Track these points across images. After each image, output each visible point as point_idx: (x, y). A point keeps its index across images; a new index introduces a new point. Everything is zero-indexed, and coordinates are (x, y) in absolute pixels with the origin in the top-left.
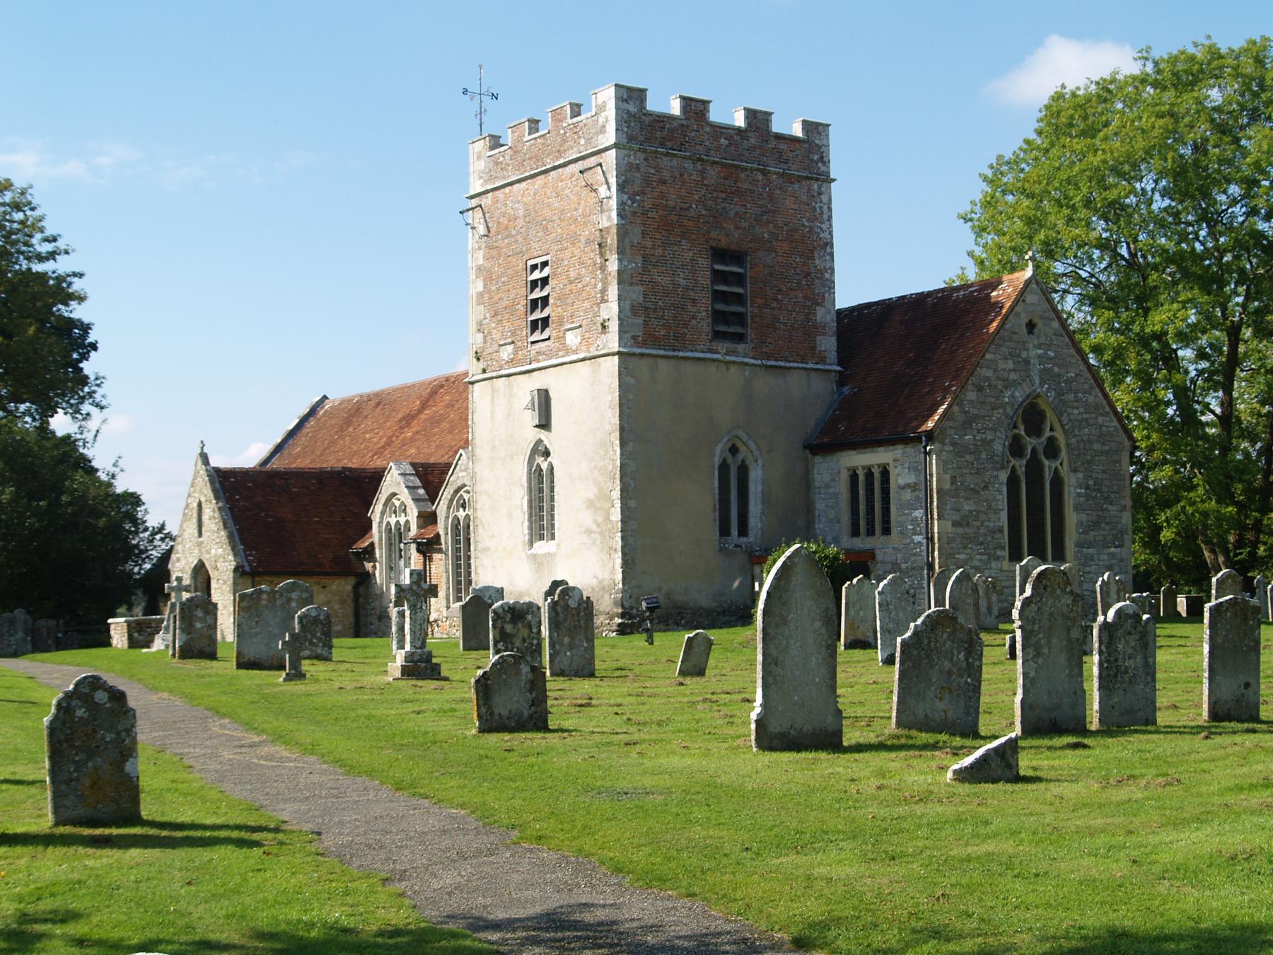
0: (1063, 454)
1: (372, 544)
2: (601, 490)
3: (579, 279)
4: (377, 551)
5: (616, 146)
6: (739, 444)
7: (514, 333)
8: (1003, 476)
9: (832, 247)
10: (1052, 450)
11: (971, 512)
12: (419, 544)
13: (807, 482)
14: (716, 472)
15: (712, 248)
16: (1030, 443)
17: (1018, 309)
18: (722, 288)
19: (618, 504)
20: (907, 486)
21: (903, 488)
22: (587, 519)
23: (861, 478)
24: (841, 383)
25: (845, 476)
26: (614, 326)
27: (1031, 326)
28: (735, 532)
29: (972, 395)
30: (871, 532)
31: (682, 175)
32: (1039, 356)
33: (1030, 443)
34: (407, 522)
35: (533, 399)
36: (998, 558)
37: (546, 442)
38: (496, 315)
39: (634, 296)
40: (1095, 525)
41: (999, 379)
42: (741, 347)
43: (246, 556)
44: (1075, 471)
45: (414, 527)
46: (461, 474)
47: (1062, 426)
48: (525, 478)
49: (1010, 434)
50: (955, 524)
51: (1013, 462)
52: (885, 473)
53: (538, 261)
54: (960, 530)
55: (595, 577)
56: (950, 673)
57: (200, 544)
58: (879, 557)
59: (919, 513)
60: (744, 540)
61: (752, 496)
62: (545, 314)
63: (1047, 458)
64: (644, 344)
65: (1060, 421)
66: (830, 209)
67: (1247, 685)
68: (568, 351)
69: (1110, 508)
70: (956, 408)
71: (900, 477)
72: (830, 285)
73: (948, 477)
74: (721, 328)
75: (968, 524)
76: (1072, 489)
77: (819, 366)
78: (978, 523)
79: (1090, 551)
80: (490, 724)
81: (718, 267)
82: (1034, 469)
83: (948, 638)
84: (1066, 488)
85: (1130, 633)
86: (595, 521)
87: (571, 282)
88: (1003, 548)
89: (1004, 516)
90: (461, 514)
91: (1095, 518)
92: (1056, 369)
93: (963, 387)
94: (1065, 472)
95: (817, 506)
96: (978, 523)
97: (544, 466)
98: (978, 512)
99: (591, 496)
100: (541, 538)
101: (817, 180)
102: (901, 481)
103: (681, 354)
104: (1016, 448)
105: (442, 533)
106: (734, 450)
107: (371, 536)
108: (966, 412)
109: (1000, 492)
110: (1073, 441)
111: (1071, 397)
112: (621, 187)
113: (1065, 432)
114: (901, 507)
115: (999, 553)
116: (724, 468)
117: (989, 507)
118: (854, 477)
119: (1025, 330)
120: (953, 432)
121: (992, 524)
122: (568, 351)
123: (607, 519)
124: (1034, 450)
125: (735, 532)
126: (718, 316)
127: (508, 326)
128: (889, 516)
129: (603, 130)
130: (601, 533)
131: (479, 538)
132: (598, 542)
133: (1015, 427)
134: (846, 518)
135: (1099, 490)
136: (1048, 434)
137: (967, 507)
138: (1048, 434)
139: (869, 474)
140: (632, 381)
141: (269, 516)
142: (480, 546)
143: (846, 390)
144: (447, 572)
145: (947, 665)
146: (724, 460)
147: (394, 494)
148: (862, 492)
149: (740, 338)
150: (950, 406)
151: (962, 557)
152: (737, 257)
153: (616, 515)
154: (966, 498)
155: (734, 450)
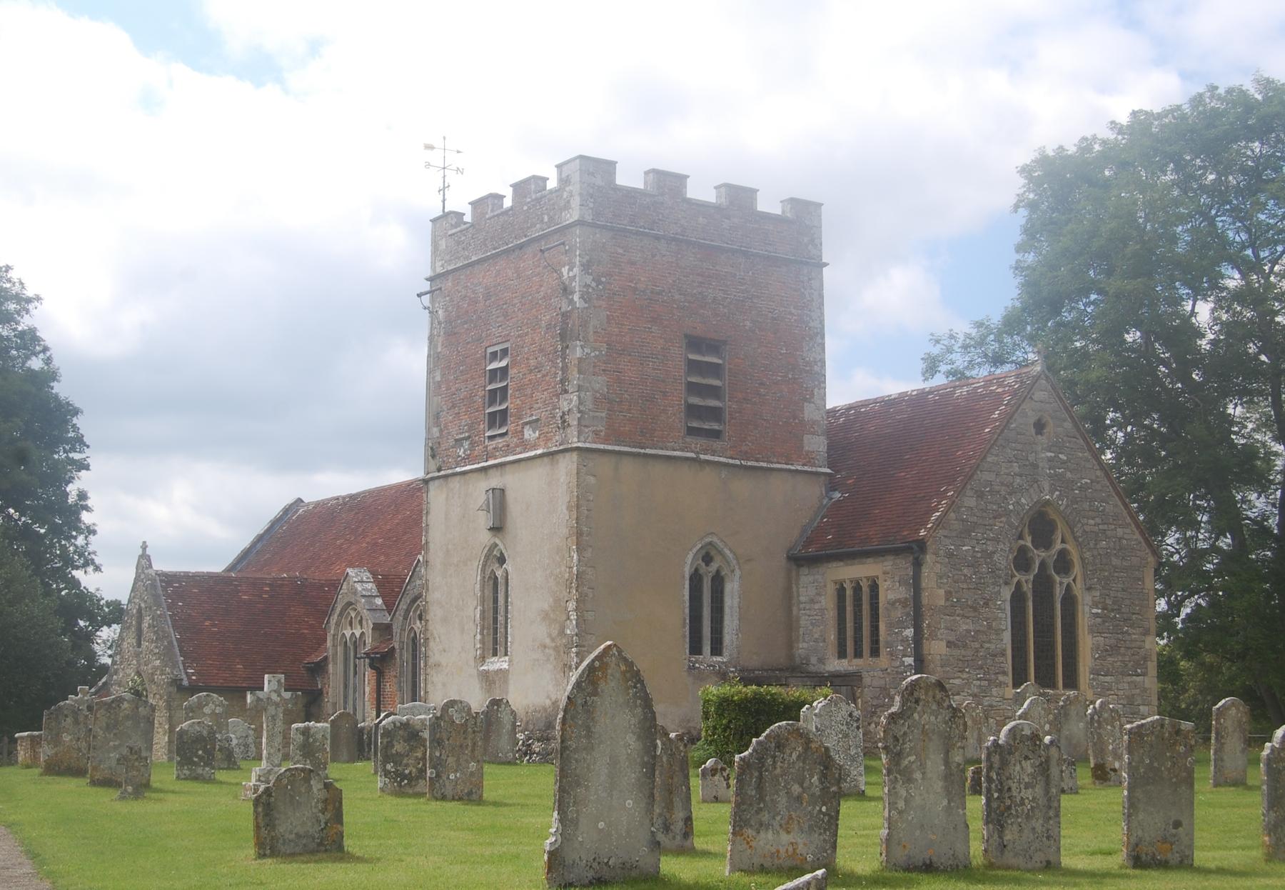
0: (1077, 570)
1: (326, 658)
2: (557, 601)
3: (538, 368)
4: (330, 666)
5: (580, 223)
6: (713, 553)
7: (471, 427)
8: (1007, 593)
9: (823, 337)
10: (1063, 564)
11: (968, 631)
12: (372, 659)
13: (788, 596)
14: (687, 583)
15: (686, 336)
16: (1038, 555)
17: (1023, 406)
18: (693, 379)
19: (573, 617)
20: (899, 600)
21: (893, 603)
22: (541, 632)
23: (849, 592)
24: (832, 487)
25: (831, 589)
26: (573, 420)
27: (1040, 427)
28: (707, 648)
29: (970, 501)
30: (858, 654)
31: (653, 256)
32: (1050, 460)
33: (1038, 555)
34: (363, 634)
35: (488, 499)
36: (1000, 684)
37: (501, 546)
38: (454, 406)
39: (597, 386)
40: (1113, 650)
41: (1002, 484)
42: (717, 445)
43: (185, 669)
44: (1089, 589)
45: (369, 640)
47: (1075, 538)
48: (478, 586)
49: (1015, 548)
50: (950, 644)
51: (1018, 577)
52: (874, 588)
53: (497, 348)
54: (956, 652)
55: (548, 697)
56: (799, 799)
57: (137, 655)
58: (867, 680)
59: (909, 632)
60: (719, 659)
61: (727, 610)
62: (503, 407)
63: (1058, 573)
64: (606, 441)
65: (1073, 532)
66: (821, 296)
67: (1177, 824)
68: (526, 446)
69: (1131, 631)
70: (952, 515)
71: (890, 592)
72: (820, 380)
73: (942, 592)
74: (695, 424)
75: (965, 646)
76: (1087, 609)
77: (806, 468)
78: (977, 645)
79: (1108, 679)
80: (268, 846)
81: (691, 357)
82: (1043, 586)
83: (799, 757)
84: (1080, 608)
85: (1026, 758)
86: (550, 635)
87: (531, 371)
88: (1005, 673)
89: (1007, 637)
90: (418, 625)
91: (1113, 641)
92: (1069, 475)
93: (960, 492)
94: (1078, 589)
95: (802, 623)
96: (977, 645)
97: (499, 573)
98: (977, 632)
99: (546, 607)
100: (495, 654)
101: (807, 263)
102: (891, 596)
103: (648, 451)
104: (1022, 561)
105: (397, 647)
106: (708, 559)
107: (326, 650)
108: (963, 520)
109: (1003, 610)
110: (1087, 555)
111: (1086, 505)
112: (586, 267)
113: (1079, 545)
114: (890, 626)
115: (1001, 678)
116: (696, 579)
117: (990, 627)
118: (841, 592)
119: (1033, 431)
120: (948, 541)
121: (993, 646)
123: (562, 633)
124: (1043, 565)
125: (707, 648)
126: (692, 411)
127: (465, 420)
128: (878, 635)
129: (567, 206)
130: (556, 649)
131: (430, 653)
132: (552, 658)
133: (1021, 537)
134: (832, 637)
135: (1119, 611)
136: (1058, 546)
137: (964, 626)
138: (1058, 546)
139: (857, 589)
140: (592, 480)
141: (214, 625)
142: (431, 661)
143: (837, 495)
144: (401, 689)
145: (796, 789)
146: (696, 570)
147: (349, 604)
148: (849, 609)
149: (716, 435)
150: (945, 514)
151: (957, 681)
152: (714, 347)
154: (964, 616)
155: (708, 559)
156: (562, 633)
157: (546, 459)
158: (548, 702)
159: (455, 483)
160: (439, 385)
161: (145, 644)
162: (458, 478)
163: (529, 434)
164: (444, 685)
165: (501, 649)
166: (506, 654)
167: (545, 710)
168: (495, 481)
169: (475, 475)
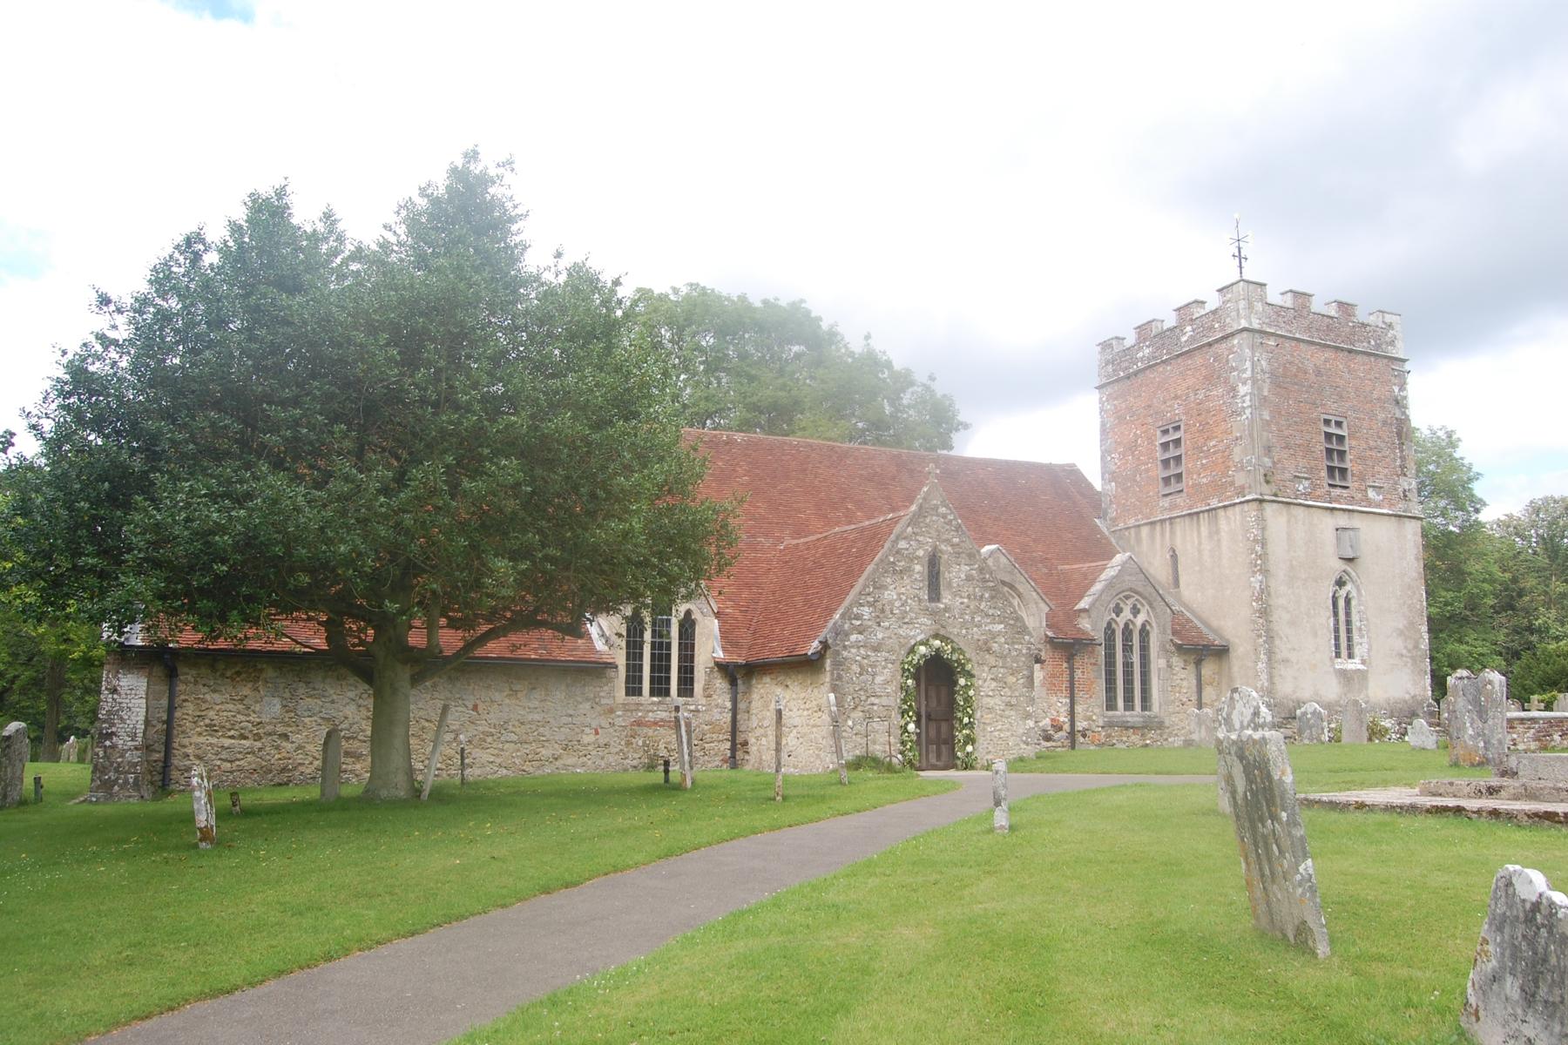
19: (1426, 636)
22: (1399, 644)
57: (933, 614)
68: (1370, 503)
122: (1370, 503)
123: (1416, 647)
130: (1413, 658)
142: (1279, 657)
153: (1425, 644)
156: (1416, 647)
159: (1300, 511)
160: (1268, 423)
161: (947, 598)
163: (1371, 494)
166: (1350, 656)
168: (1343, 520)
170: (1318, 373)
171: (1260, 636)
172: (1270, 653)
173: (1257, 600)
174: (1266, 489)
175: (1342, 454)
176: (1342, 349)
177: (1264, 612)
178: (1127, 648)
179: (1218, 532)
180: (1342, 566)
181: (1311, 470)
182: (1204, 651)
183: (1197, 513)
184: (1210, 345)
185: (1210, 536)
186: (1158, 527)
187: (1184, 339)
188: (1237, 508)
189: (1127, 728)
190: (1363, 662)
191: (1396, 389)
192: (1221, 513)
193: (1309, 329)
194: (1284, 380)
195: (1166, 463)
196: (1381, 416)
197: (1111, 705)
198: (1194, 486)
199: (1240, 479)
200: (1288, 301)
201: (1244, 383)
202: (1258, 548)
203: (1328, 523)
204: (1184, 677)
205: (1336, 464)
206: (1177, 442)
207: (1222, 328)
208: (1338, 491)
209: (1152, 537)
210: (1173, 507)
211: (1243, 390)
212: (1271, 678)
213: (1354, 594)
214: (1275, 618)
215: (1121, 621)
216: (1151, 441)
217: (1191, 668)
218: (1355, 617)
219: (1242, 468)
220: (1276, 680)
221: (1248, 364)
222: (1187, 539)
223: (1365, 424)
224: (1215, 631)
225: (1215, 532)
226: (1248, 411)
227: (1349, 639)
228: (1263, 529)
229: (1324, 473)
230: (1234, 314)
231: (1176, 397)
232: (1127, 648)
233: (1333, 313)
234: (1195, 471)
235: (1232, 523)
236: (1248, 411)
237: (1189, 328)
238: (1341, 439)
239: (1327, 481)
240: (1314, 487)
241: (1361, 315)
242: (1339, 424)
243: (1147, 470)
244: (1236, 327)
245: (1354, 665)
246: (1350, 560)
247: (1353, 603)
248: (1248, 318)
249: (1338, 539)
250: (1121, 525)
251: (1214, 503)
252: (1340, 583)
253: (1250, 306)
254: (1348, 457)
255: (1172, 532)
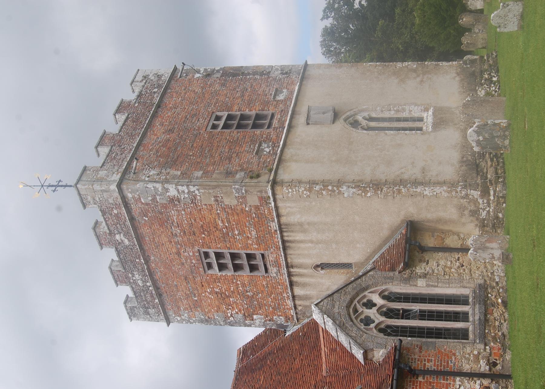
19: (406, 64)
46: (336, 310)
55: (454, 78)
68: (289, 98)
86: (415, 78)
122: (289, 98)
132: (430, 76)
142: (419, 176)
156: (415, 71)
157: (304, 82)
158: (458, 79)
159: (289, 152)
160: (206, 173)
162: (286, 150)
163: (281, 97)
164: (440, 163)
165: (417, 124)
167: (462, 80)
168: (301, 119)
169: (290, 136)
170: (171, 131)
171: (399, 191)
172: (416, 183)
173: (366, 192)
174: (264, 178)
175: (243, 117)
176: (156, 112)
177: (377, 186)
178: (406, 314)
179: (301, 224)
180: (340, 124)
181: (253, 142)
182: (412, 245)
183: (284, 242)
184: (132, 219)
185: (304, 231)
186: (295, 279)
187: (126, 242)
188: (280, 204)
189: (486, 320)
190: (427, 110)
191: (197, 75)
192: (283, 220)
193: (132, 136)
194: (174, 158)
195: (237, 268)
196: (217, 87)
197: (463, 335)
198: (259, 244)
199: (253, 200)
200: (104, 150)
201: (167, 190)
202: (317, 188)
203: (302, 130)
204: (436, 263)
205: (251, 122)
206: (219, 256)
207: (117, 207)
208: (275, 123)
209: (304, 285)
210: (277, 264)
211: (172, 192)
212: (441, 184)
213: (366, 114)
214: (383, 178)
215: (379, 319)
216: (217, 280)
217: (427, 256)
218: (387, 115)
219: (244, 197)
220: (441, 179)
221: (150, 185)
222: (305, 254)
223: (222, 98)
224: (393, 232)
225: (302, 227)
226: (192, 189)
227: (406, 120)
228: (300, 182)
229: (258, 132)
230: (105, 195)
231: (178, 253)
232: (406, 314)
233: (124, 117)
234: (245, 242)
235: (293, 210)
236: (192, 189)
237: (118, 237)
238: (230, 117)
239: (265, 130)
240: (268, 139)
241: (131, 97)
242: (218, 118)
243: (243, 285)
244: (116, 194)
245: (429, 117)
246: (336, 116)
247: (374, 115)
248: (110, 183)
249: (316, 123)
250: (292, 312)
251: (274, 226)
252: (355, 124)
253: (101, 180)
254: (247, 112)
255: (300, 266)
